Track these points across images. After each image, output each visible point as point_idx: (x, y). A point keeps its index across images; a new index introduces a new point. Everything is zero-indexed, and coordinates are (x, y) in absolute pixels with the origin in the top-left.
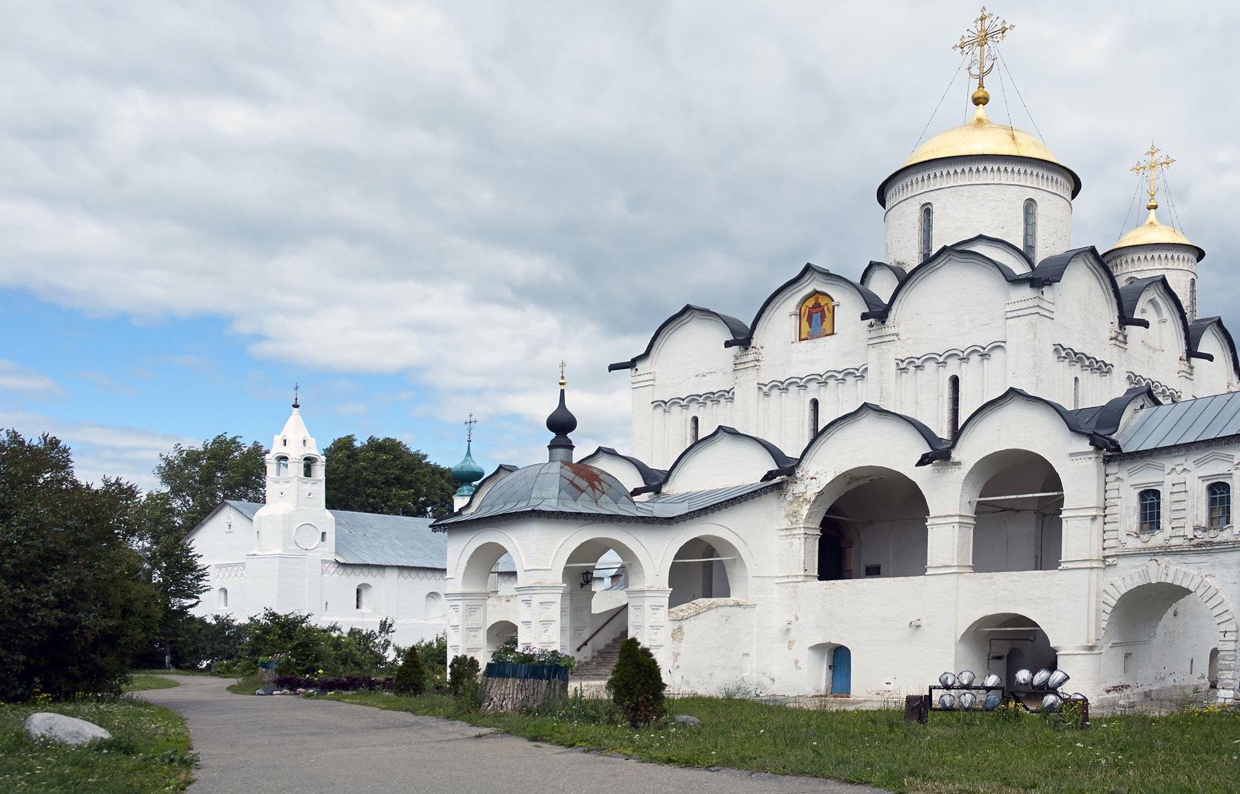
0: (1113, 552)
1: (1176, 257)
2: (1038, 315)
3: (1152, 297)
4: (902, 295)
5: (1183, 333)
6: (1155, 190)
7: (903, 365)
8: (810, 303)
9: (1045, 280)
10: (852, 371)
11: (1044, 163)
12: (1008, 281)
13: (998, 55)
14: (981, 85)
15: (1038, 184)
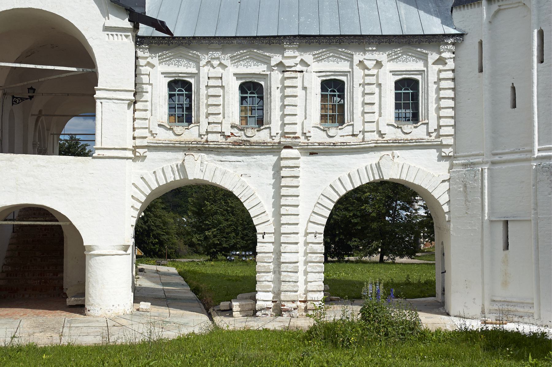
0: (145, 143)
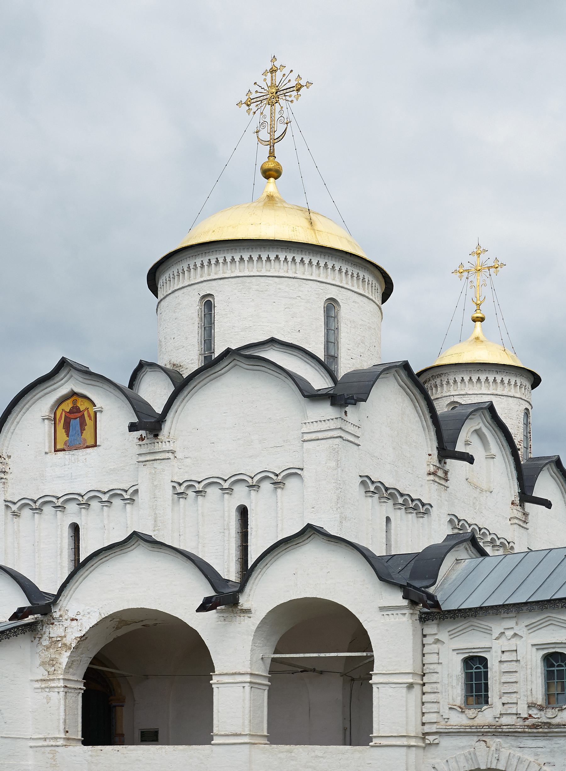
0: (434, 728)
1: (506, 381)
2: (341, 439)
3: (477, 427)
4: (178, 404)
5: (515, 473)
6: (482, 299)
7: (181, 489)
8: (67, 406)
9: (348, 398)
10: (119, 492)
11: (348, 257)
12: (305, 396)
13: (291, 118)
14: (272, 154)
15: (341, 282)
